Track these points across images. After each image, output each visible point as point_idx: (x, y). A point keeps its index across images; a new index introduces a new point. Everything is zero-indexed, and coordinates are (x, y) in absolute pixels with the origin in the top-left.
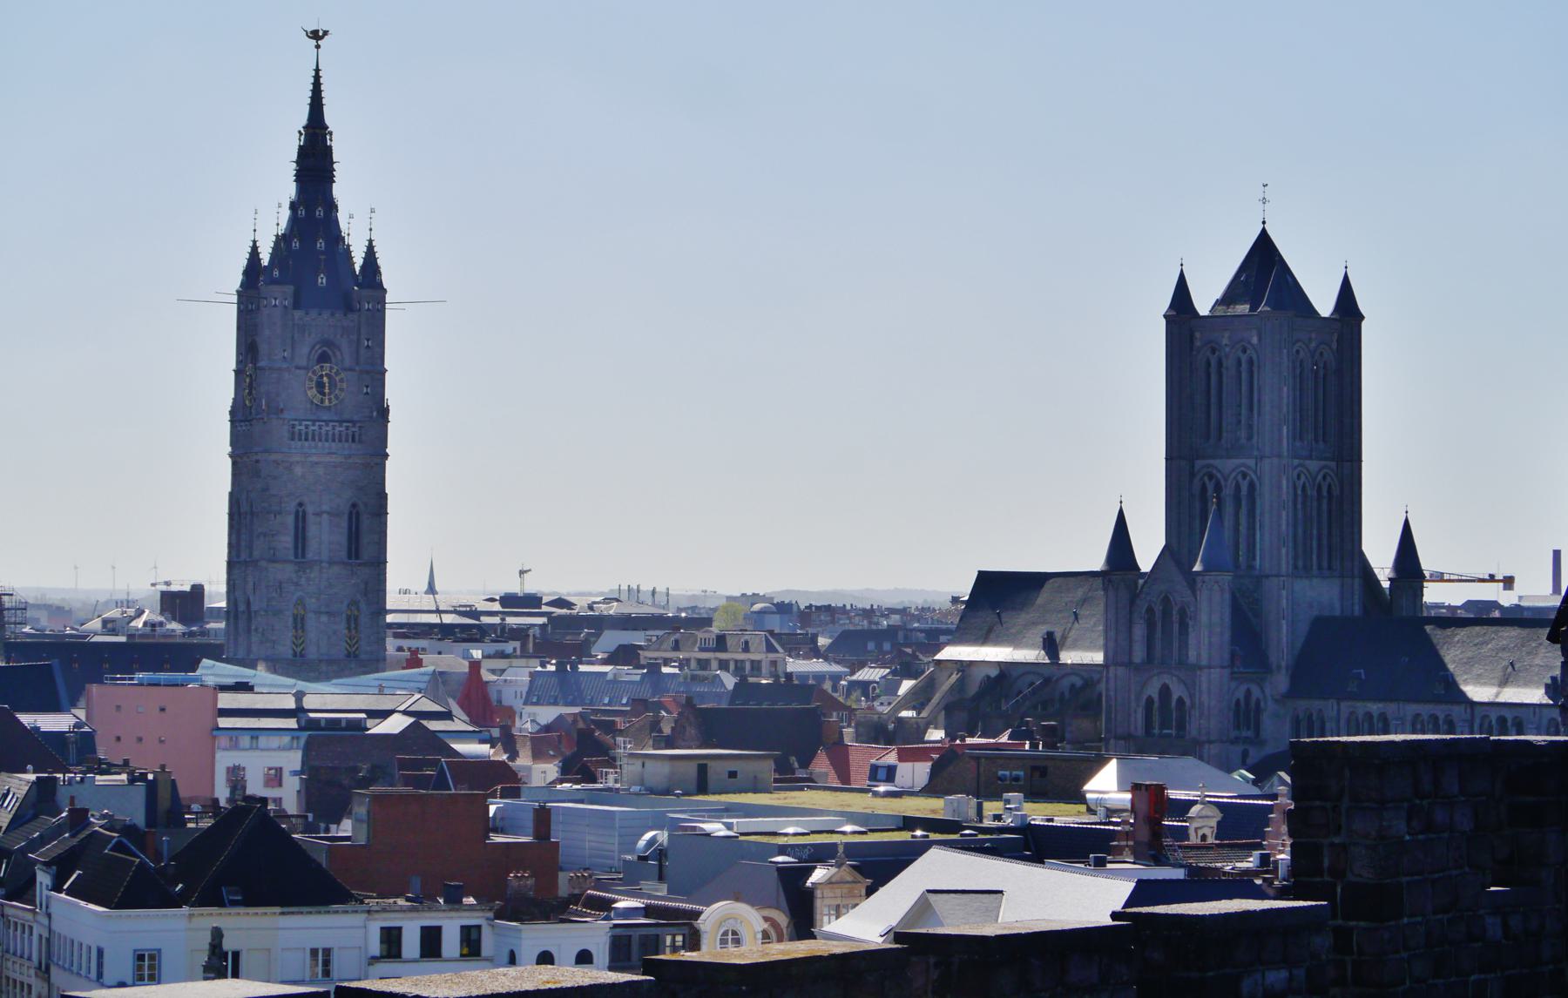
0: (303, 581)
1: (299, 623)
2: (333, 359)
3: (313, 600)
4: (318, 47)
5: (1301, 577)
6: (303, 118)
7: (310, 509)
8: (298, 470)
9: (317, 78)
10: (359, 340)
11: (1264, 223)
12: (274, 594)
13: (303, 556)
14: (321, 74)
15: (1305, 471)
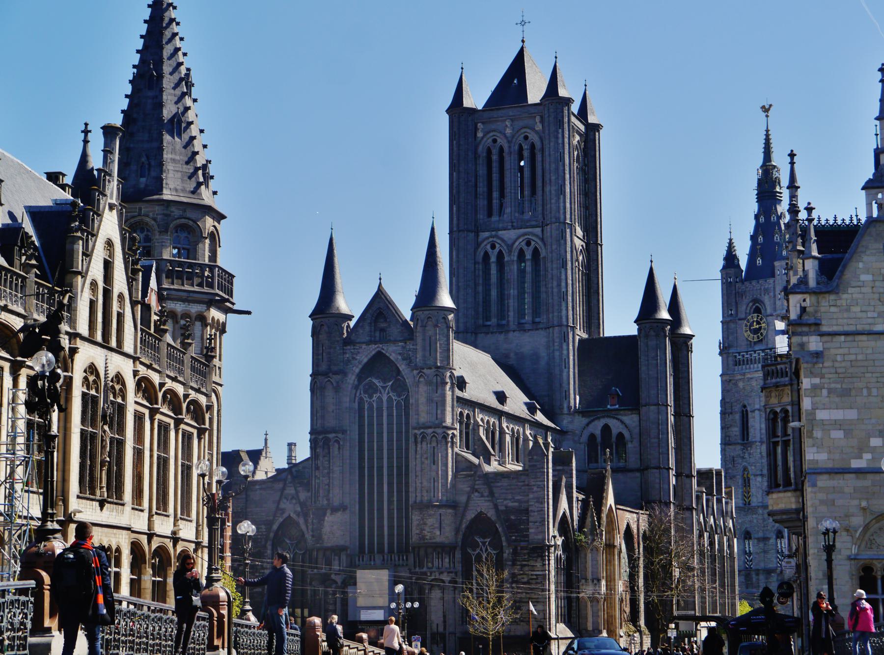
0: (746, 456)
1: (746, 483)
2: (763, 311)
3: (753, 468)
4: (767, 116)
5: (492, 333)
6: (760, 162)
7: (749, 409)
8: (741, 384)
9: (767, 136)
10: (775, 296)
11: (523, 41)
12: (730, 466)
13: (748, 439)
14: (770, 133)
15: (499, 241)
